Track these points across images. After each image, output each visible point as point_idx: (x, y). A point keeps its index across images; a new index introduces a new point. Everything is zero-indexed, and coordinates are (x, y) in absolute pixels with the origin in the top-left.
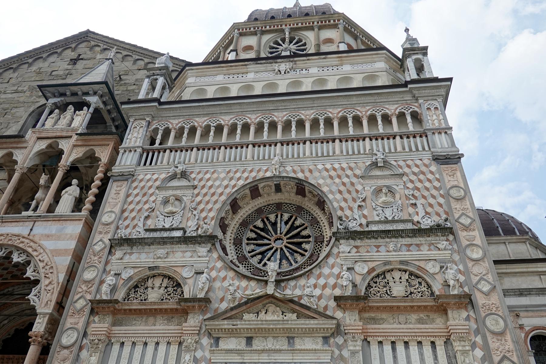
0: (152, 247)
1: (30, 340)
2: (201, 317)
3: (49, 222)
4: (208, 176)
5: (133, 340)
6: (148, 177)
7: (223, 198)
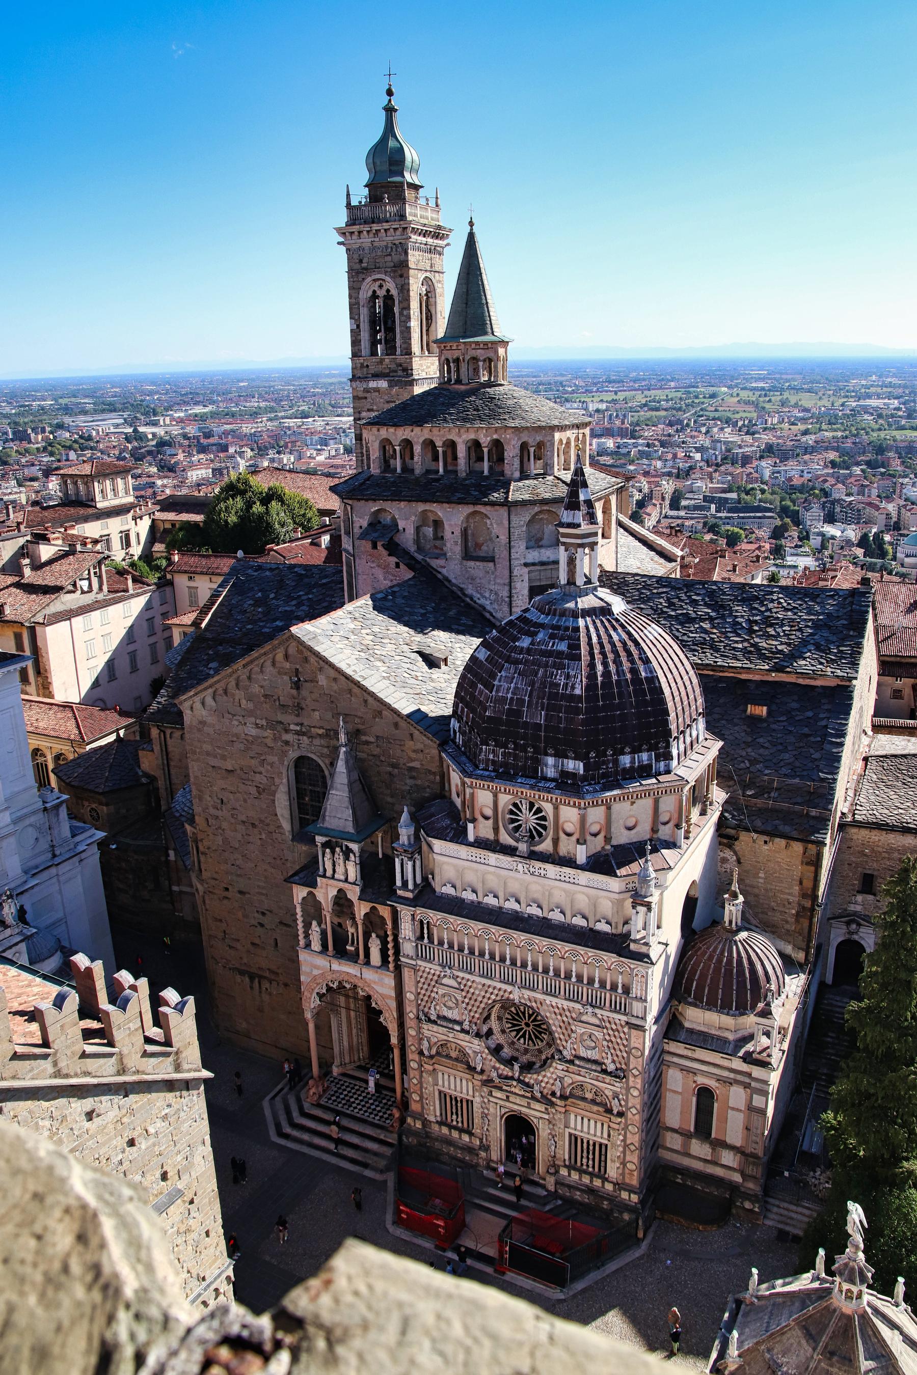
4: (469, 983)
6: (427, 970)
7: (483, 1005)
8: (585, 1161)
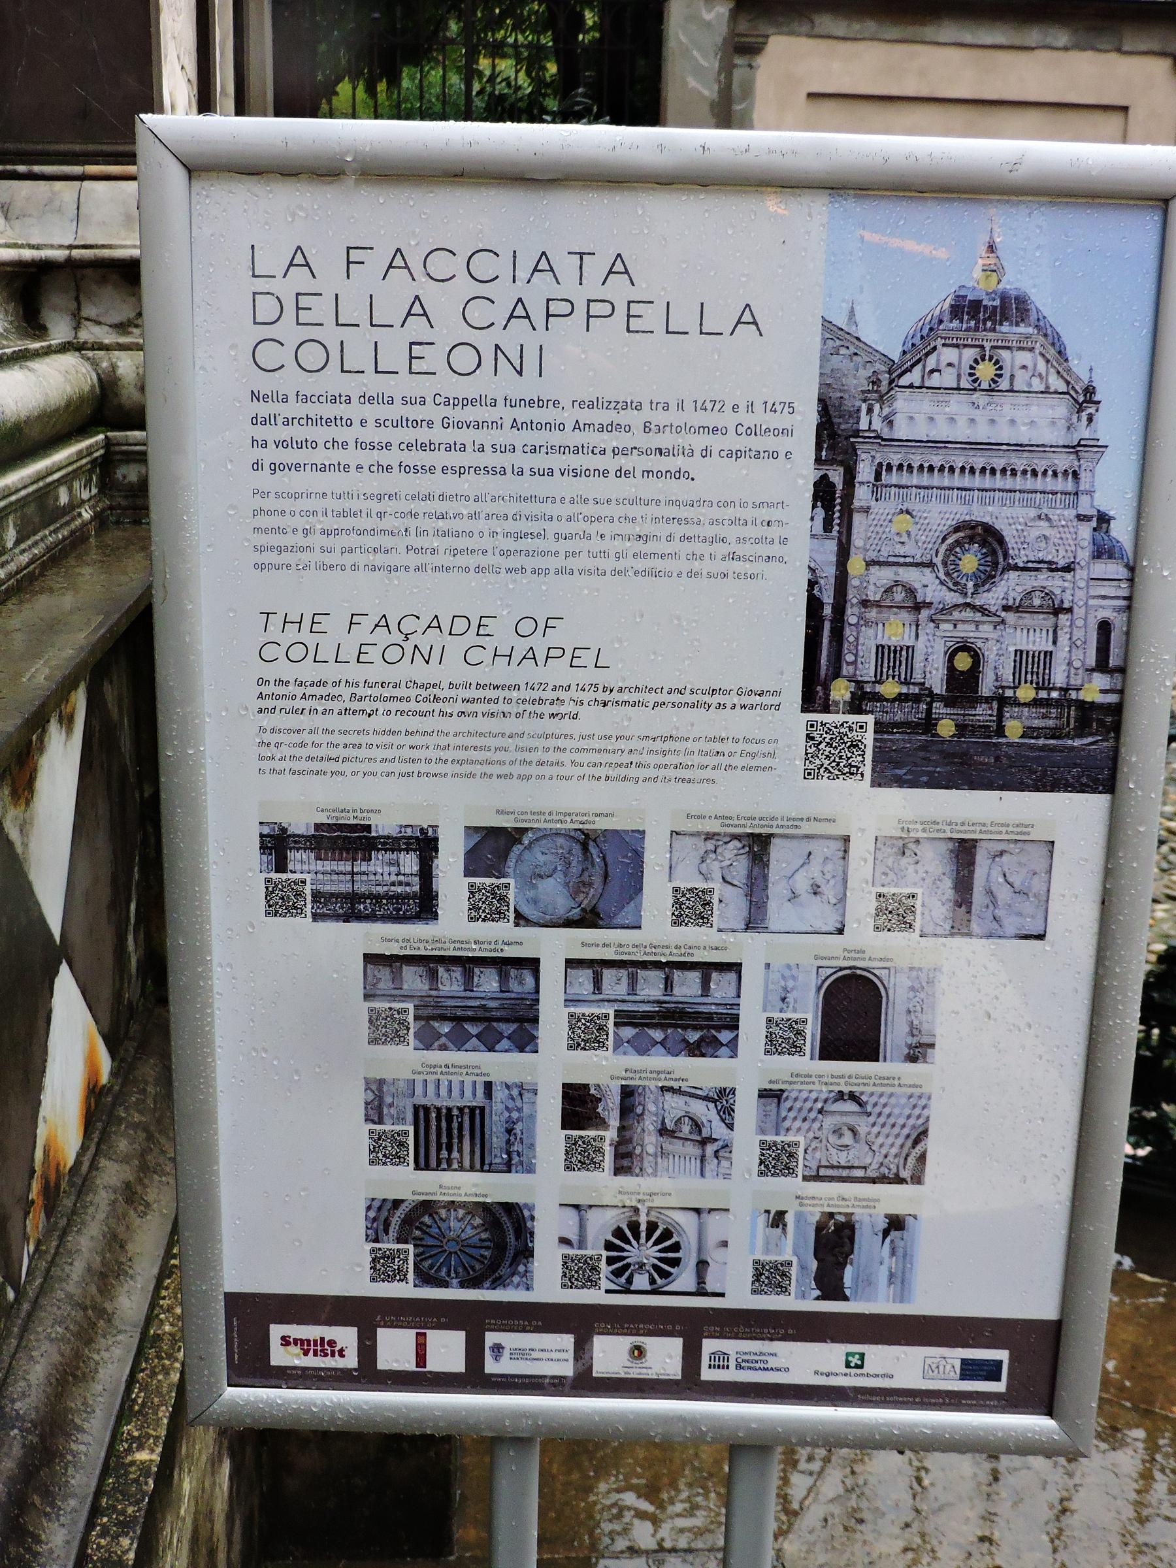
8: (1029, 676)
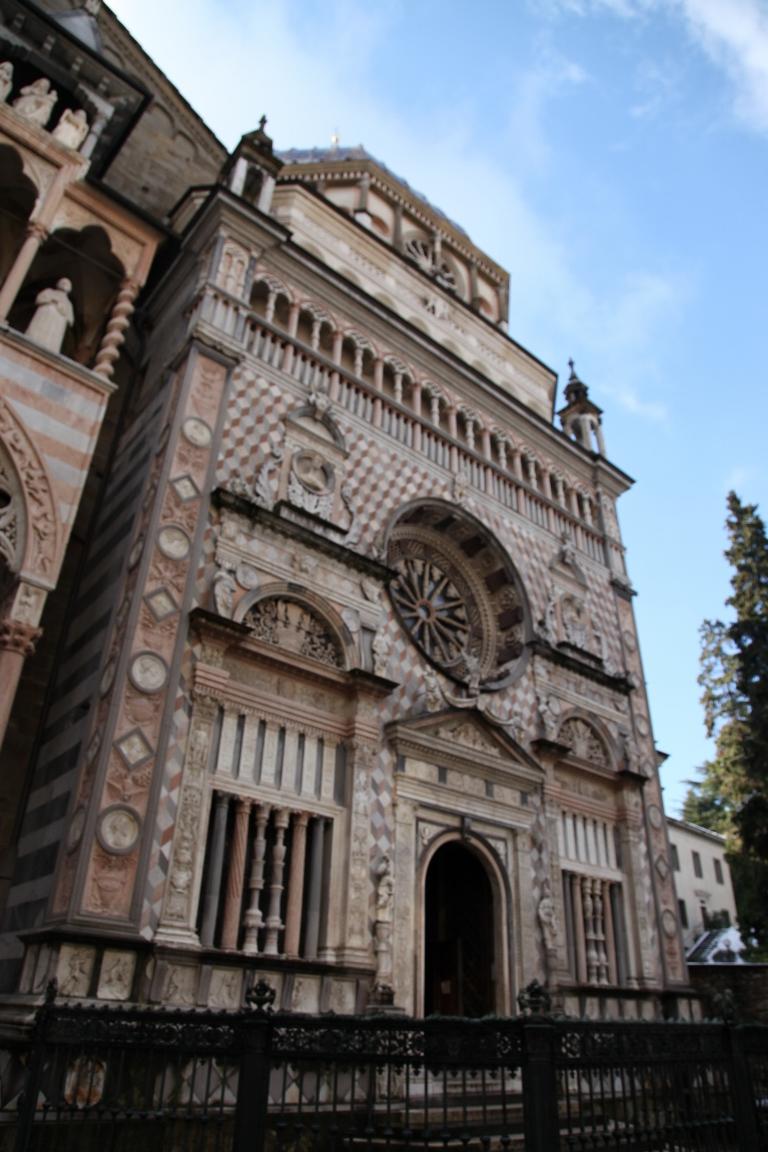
0: (290, 541)
1: (7, 638)
2: (375, 713)
3: (23, 358)
5: (263, 716)
6: (263, 383)
7: (389, 503)
